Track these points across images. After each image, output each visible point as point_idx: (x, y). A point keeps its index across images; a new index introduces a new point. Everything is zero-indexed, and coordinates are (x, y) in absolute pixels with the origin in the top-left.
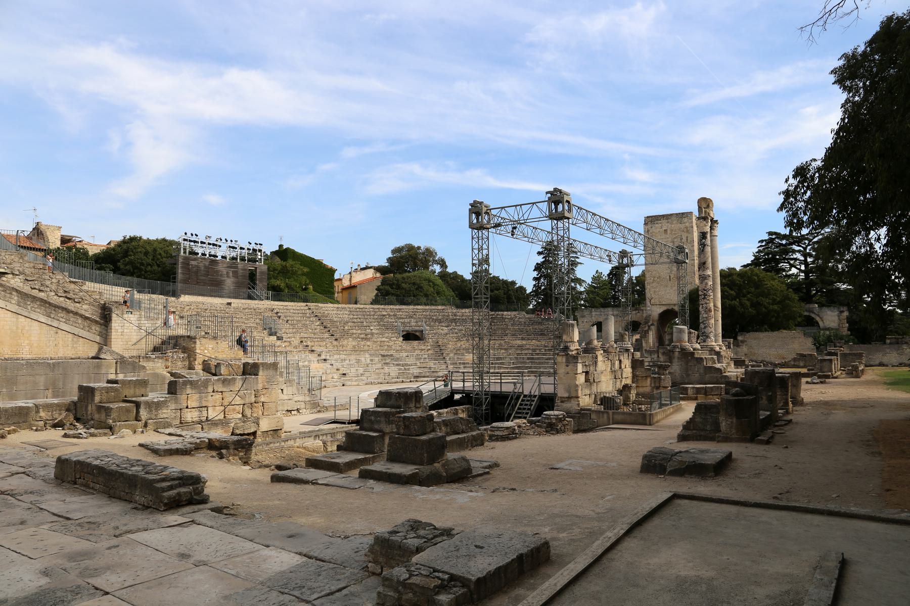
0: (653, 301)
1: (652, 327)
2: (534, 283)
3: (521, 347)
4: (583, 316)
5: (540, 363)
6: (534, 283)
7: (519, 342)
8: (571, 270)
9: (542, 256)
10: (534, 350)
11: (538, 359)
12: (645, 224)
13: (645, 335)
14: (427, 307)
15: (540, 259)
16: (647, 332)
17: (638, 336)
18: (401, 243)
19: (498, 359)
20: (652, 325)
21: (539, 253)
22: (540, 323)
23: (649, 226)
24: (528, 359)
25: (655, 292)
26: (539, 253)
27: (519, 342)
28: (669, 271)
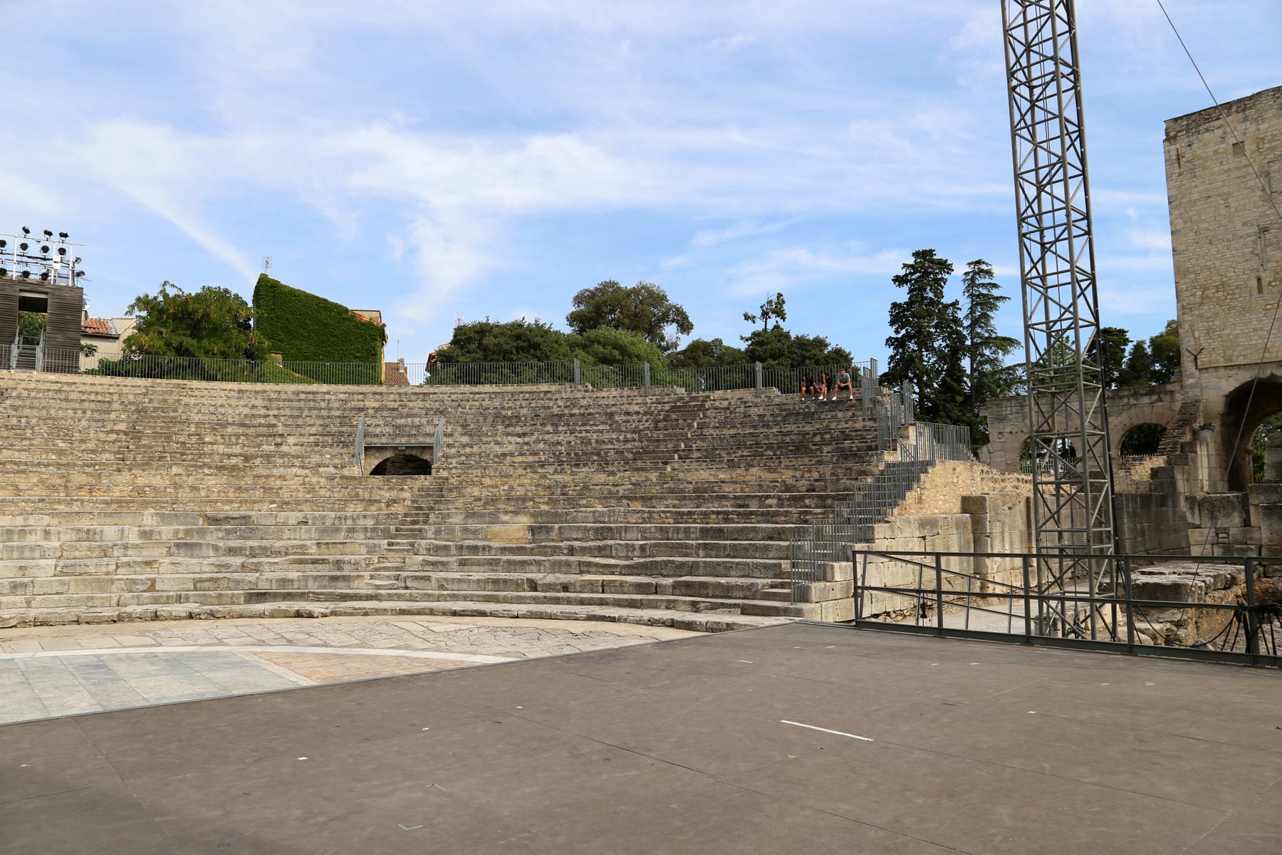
0: (1203, 359)
1: (1206, 434)
2: (891, 351)
3: (702, 492)
4: (1001, 419)
5: (736, 552)
6: (891, 351)
7: (704, 474)
8: (979, 320)
9: (906, 288)
10: (742, 501)
11: (740, 534)
12: (1169, 139)
13: (1183, 456)
14: (510, 388)
15: (902, 295)
16: (1191, 446)
17: (1158, 461)
18: (592, 283)
19: (602, 533)
20: (1207, 426)
21: (899, 280)
22: (808, 416)
23: (1181, 144)
24: (705, 533)
25: (1209, 331)
26: (899, 280)
27: (704, 474)
28: (1255, 263)
